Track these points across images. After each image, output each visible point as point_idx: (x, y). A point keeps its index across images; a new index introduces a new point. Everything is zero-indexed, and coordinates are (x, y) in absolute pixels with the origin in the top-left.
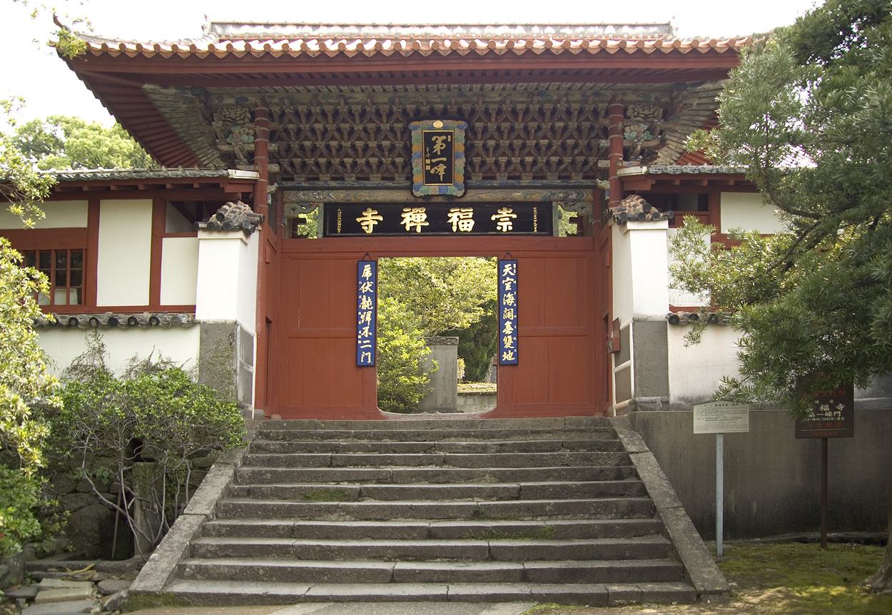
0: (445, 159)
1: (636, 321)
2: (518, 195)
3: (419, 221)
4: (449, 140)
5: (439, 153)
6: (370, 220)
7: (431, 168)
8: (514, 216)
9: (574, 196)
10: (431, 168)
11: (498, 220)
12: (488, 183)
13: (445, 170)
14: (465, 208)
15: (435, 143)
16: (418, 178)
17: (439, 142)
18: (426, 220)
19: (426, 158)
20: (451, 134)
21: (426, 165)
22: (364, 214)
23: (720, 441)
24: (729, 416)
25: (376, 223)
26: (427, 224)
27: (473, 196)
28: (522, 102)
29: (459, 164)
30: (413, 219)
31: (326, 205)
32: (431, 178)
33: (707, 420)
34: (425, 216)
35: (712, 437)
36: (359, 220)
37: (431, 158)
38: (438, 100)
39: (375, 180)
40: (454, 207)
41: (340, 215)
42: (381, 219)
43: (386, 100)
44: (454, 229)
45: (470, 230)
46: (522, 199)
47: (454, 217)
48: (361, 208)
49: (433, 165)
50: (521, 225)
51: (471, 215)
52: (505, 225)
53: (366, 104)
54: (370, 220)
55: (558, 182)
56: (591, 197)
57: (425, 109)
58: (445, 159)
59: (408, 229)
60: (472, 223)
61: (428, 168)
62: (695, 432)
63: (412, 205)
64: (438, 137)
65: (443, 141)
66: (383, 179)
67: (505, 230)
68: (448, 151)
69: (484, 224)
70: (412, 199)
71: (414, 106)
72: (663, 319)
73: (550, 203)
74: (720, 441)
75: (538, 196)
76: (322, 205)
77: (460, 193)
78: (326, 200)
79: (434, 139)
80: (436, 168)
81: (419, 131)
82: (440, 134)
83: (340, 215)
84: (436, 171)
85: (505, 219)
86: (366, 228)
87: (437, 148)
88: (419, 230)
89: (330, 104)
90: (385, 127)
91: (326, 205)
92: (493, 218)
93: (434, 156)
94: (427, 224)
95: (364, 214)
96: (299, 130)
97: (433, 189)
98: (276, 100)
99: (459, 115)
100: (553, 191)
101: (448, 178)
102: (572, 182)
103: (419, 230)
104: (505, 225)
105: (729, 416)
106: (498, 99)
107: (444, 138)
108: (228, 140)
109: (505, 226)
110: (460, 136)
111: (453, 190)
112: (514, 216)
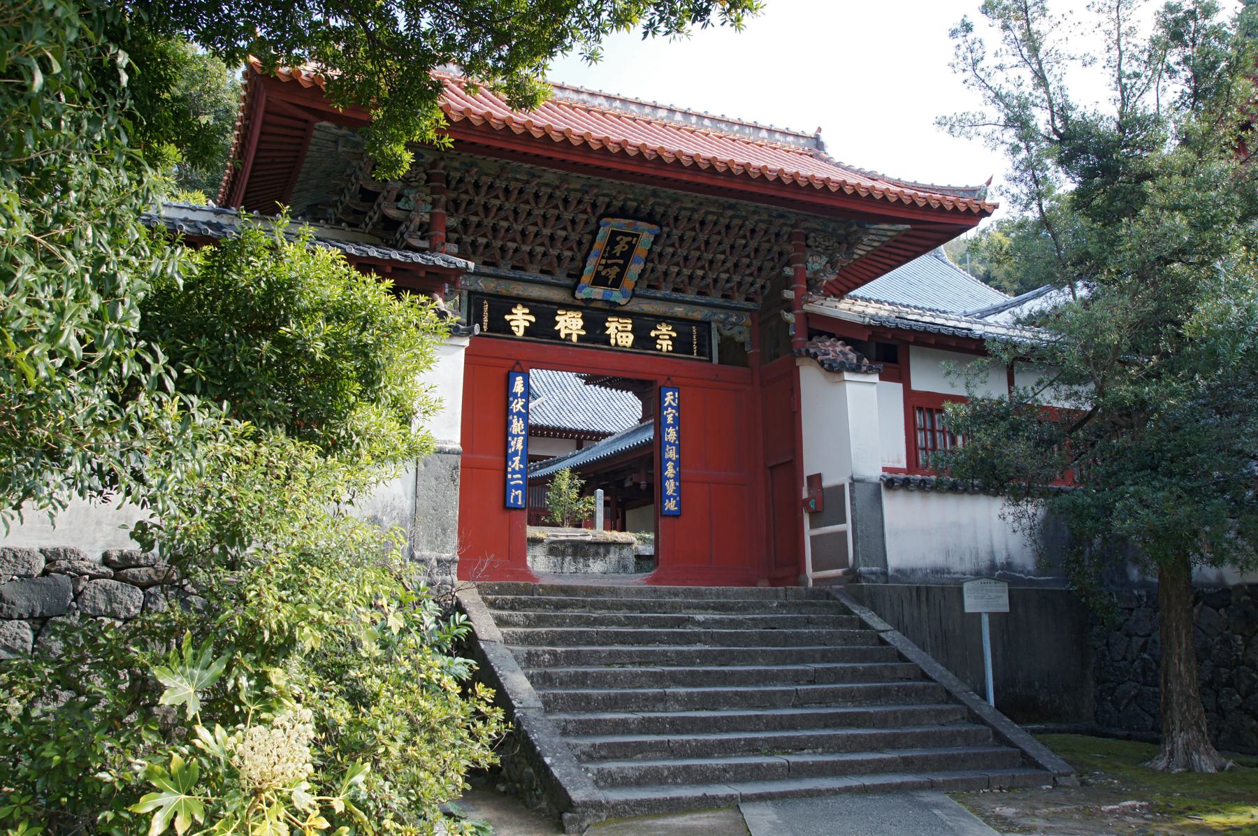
0: (621, 262)
1: (854, 481)
2: (679, 310)
3: (574, 328)
6: (520, 319)
8: (674, 335)
9: (734, 319)
11: (657, 337)
12: (651, 292)
13: (618, 274)
14: (623, 318)
15: (618, 243)
16: (587, 278)
17: (622, 244)
18: (583, 328)
20: (638, 236)
22: (514, 311)
23: (985, 620)
24: (993, 595)
25: (527, 324)
26: (583, 333)
27: (636, 306)
28: (712, 213)
29: (635, 269)
30: (568, 324)
31: (470, 293)
32: (598, 280)
33: (975, 598)
34: (581, 323)
35: (979, 614)
36: (508, 317)
37: (608, 258)
38: (631, 197)
39: (533, 273)
40: (612, 316)
41: (486, 308)
42: (533, 319)
43: (578, 187)
44: (613, 341)
45: (629, 344)
46: (683, 316)
47: (613, 326)
48: (509, 303)
49: (606, 266)
50: (680, 344)
51: (630, 327)
52: (665, 343)
53: (558, 187)
54: (520, 319)
55: (720, 301)
56: (749, 322)
57: (617, 204)
58: (621, 262)
59: (563, 336)
60: (631, 337)
61: (601, 268)
62: (967, 610)
63: (568, 307)
65: (627, 243)
66: (542, 272)
67: (665, 349)
68: (627, 256)
69: (644, 340)
70: (569, 300)
71: (607, 200)
72: (877, 480)
73: (709, 323)
74: (985, 620)
75: (699, 314)
76: (465, 293)
77: (623, 301)
78: (472, 288)
81: (606, 228)
83: (486, 308)
85: (664, 337)
86: (514, 329)
87: (618, 250)
88: (574, 338)
89: (517, 180)
90: (567, 216)
91: (470, 293)
92: (653, 334)
94: (583, 333)
95: (514, 311)
96: (470, 202)
97: (598, 292)
98: (456, 164)
99: (650, 218)
100: (715, 310)
102: (734, 303)
103: (574, 338)
104: (665, 343)
105: (993, 595)
106: (690, 205)
107: (629, 239)
108: (400, 205)
109: (665, 345)
110: (646, 240)
111: (616, 296)
112: (674, 335)
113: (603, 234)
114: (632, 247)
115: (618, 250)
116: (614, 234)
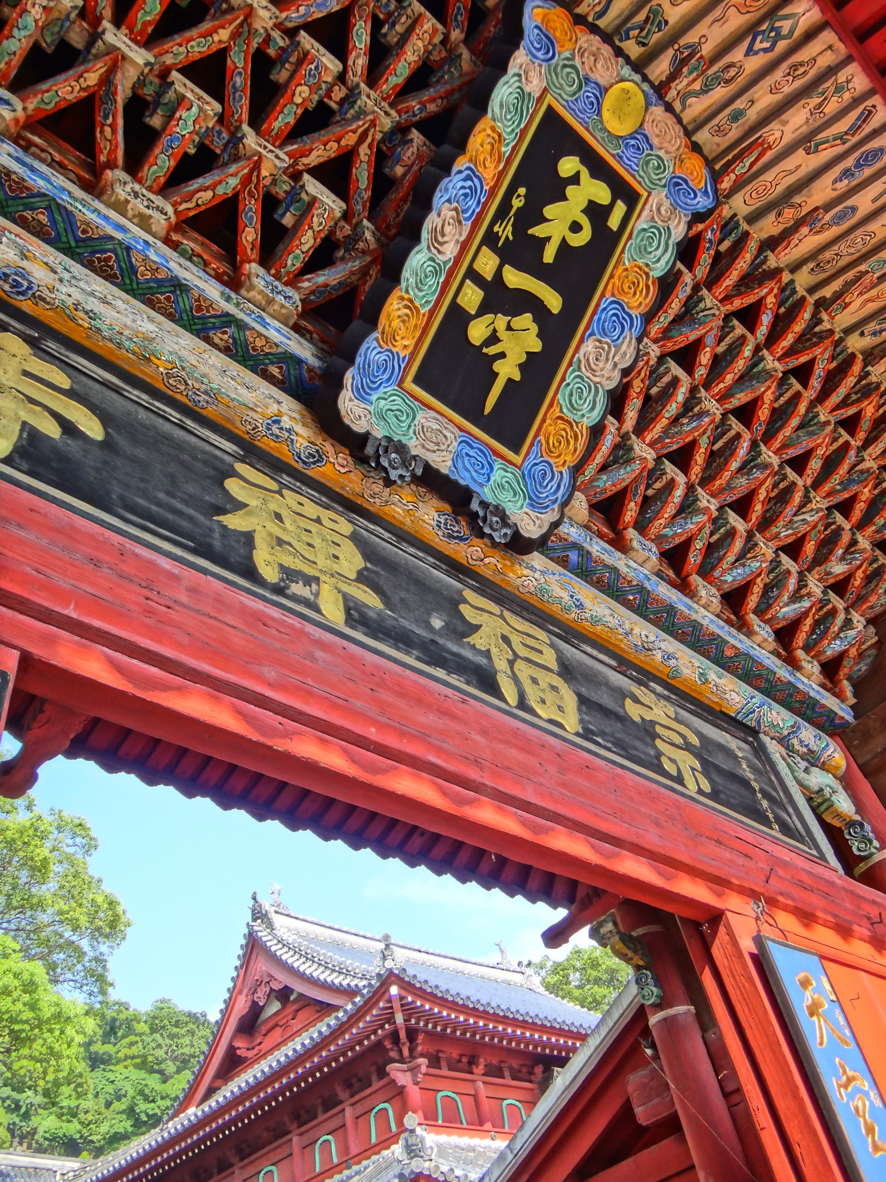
0: (554, 301)
4: (614, 222)
5: (549, 255)
7: (483, 309)
10: (483, 309)
15: (557, 190)
19: (490, 240)
21: (473, 275)
25: (52, 430)
29: (598, 361)
32: (452, 369)
42: (93, 428)
49: (500, 299)
58: (554, 301)
64: (585, 174)
68: (581, 271)
79: (568, 165)
80: (501, 321)
82: (599, 168)
84: (493, 339)
87: (561, 225)
93: (522, 251)
97: (436, 435)
101: (512, 421)
107: (601, 193)
113: (520, 89)
114: (605, 242)
115: (561, 225)
116: (554, 136)
